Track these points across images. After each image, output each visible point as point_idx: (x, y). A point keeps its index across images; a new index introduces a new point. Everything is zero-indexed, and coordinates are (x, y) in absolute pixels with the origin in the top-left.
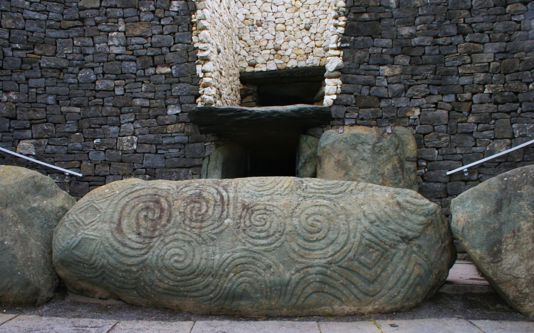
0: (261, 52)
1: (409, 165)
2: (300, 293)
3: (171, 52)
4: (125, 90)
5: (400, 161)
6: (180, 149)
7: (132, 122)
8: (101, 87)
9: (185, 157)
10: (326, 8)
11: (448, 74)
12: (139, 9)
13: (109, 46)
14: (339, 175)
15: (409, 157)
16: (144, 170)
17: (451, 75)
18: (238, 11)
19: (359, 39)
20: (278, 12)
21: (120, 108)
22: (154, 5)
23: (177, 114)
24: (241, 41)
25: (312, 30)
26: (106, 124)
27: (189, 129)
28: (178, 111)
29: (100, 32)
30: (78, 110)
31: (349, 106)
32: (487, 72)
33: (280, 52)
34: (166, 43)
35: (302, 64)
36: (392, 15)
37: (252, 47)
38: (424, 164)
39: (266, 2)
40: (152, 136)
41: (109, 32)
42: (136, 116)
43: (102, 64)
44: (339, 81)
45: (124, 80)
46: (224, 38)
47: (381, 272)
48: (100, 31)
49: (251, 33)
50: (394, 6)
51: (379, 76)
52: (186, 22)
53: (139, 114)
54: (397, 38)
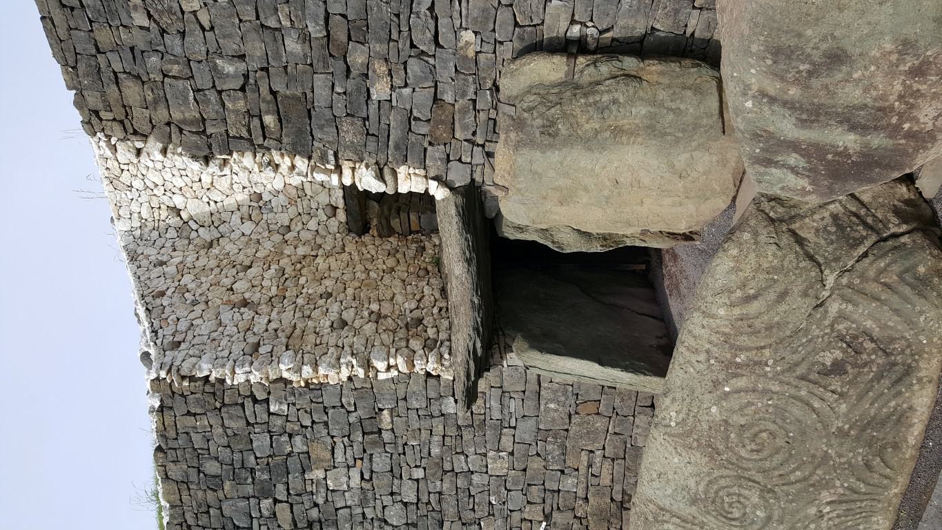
0: (308, 197)
2: (876, 476)
3: (356, 410)
4: (416, 466)
6: (511, 398)
7: (467, 456)
9: (524, 392)
12: (289, 455)
14: (585, 200)
15: (567, 75)
16: (539, 442)
18: (238, 233)
21: (445, 472)
22: (280, 435)
23: (456, 401)
24: (293, 227)
26: (469, 489)
28: (452, 399)
29: (327, 500)
31: (448, 155)
34: (343, 419)
36: (262, 69)
37: (301, 211)
39: (212, 183)
41: (328, 489)
42: (457, 453)
43: (378, 496)
44: (402, 171)
45: (401, 468)
46: (309, 299)
47: (872, 340)
49: (275, 210)
50: (242, 67)
51: (390, 101)
54: (311, 65)
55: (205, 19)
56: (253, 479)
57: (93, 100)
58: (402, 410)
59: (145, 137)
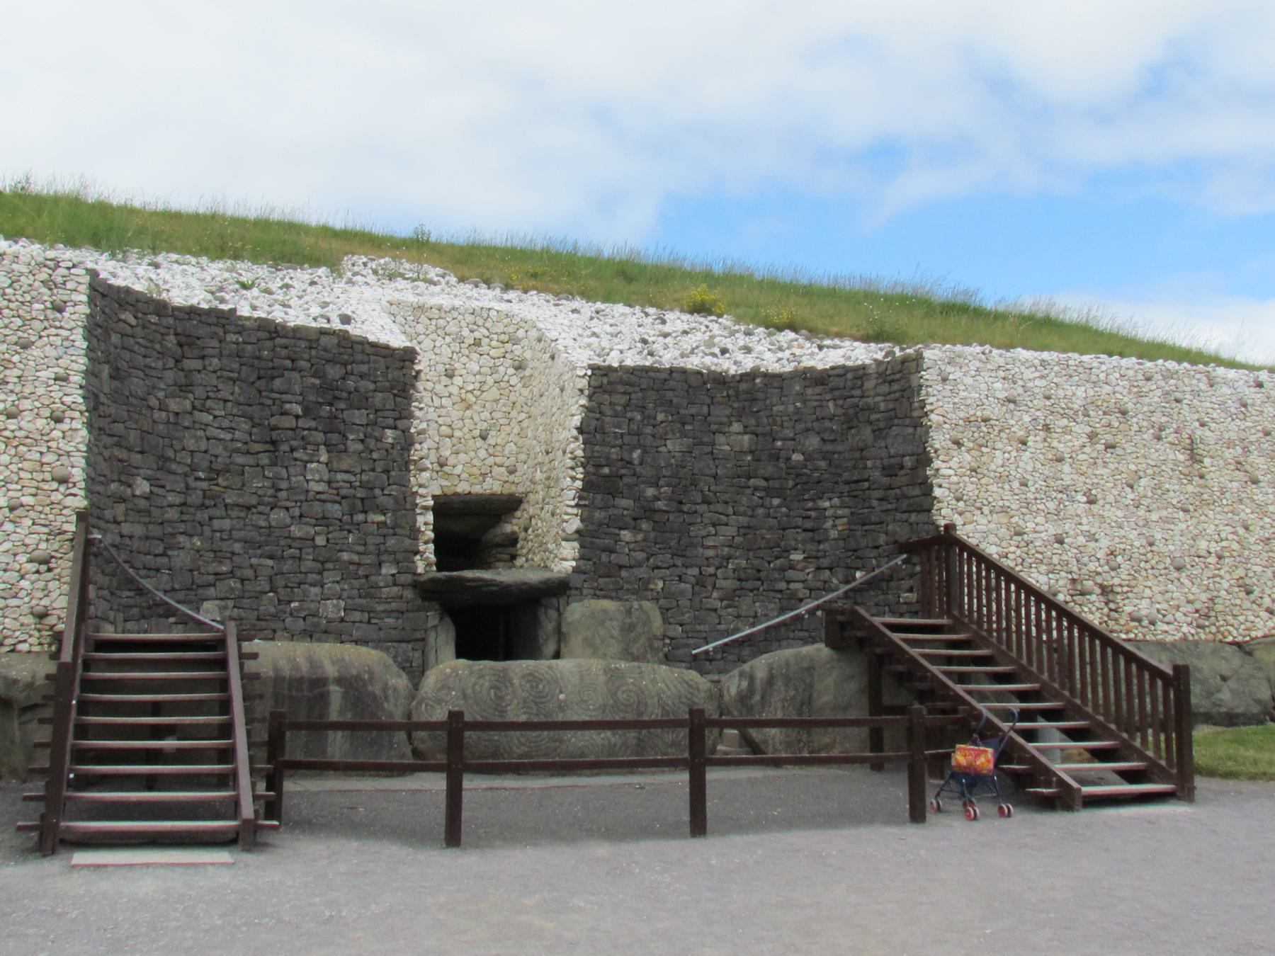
1: (657, 644)
4: (328, 540)
5: (649, 639)
8: (298, 534)
10: (508, 409)
11: (694, 546)
13: (308, 481)
17: (695, 547)
19: (599, 497)
20: (442, 407)
21: (323, 563)
23: (393, 575)
25: (491, 441)
27: (409, 594)
28: (394, 571)
30: (270, 562)
32: (730, 546)
33: (446, 469)
35: (477, 489)
38: (668, 641)
40: (363, 601)
48: (296, 459)
50: (636, 462)
52: (400, 458)
53: (347, 572)
55: (663, 449)
56: (321, 404)
57: (614, 377)
58: (385, 531)
59: (590, 397)
